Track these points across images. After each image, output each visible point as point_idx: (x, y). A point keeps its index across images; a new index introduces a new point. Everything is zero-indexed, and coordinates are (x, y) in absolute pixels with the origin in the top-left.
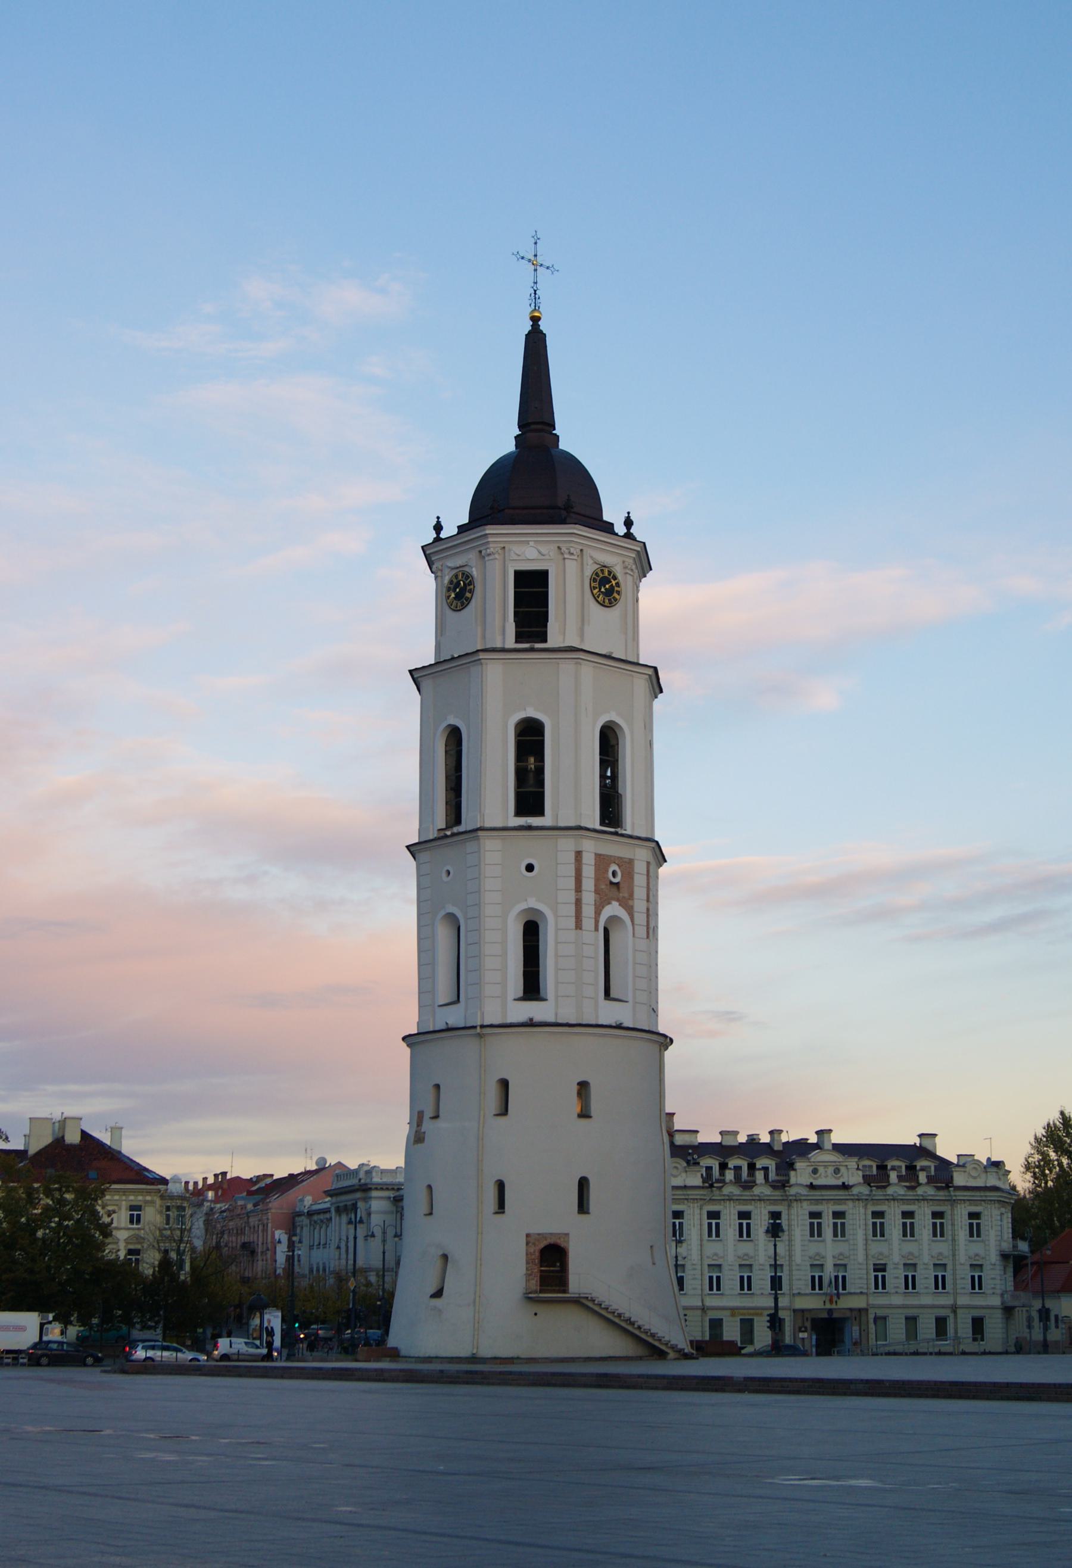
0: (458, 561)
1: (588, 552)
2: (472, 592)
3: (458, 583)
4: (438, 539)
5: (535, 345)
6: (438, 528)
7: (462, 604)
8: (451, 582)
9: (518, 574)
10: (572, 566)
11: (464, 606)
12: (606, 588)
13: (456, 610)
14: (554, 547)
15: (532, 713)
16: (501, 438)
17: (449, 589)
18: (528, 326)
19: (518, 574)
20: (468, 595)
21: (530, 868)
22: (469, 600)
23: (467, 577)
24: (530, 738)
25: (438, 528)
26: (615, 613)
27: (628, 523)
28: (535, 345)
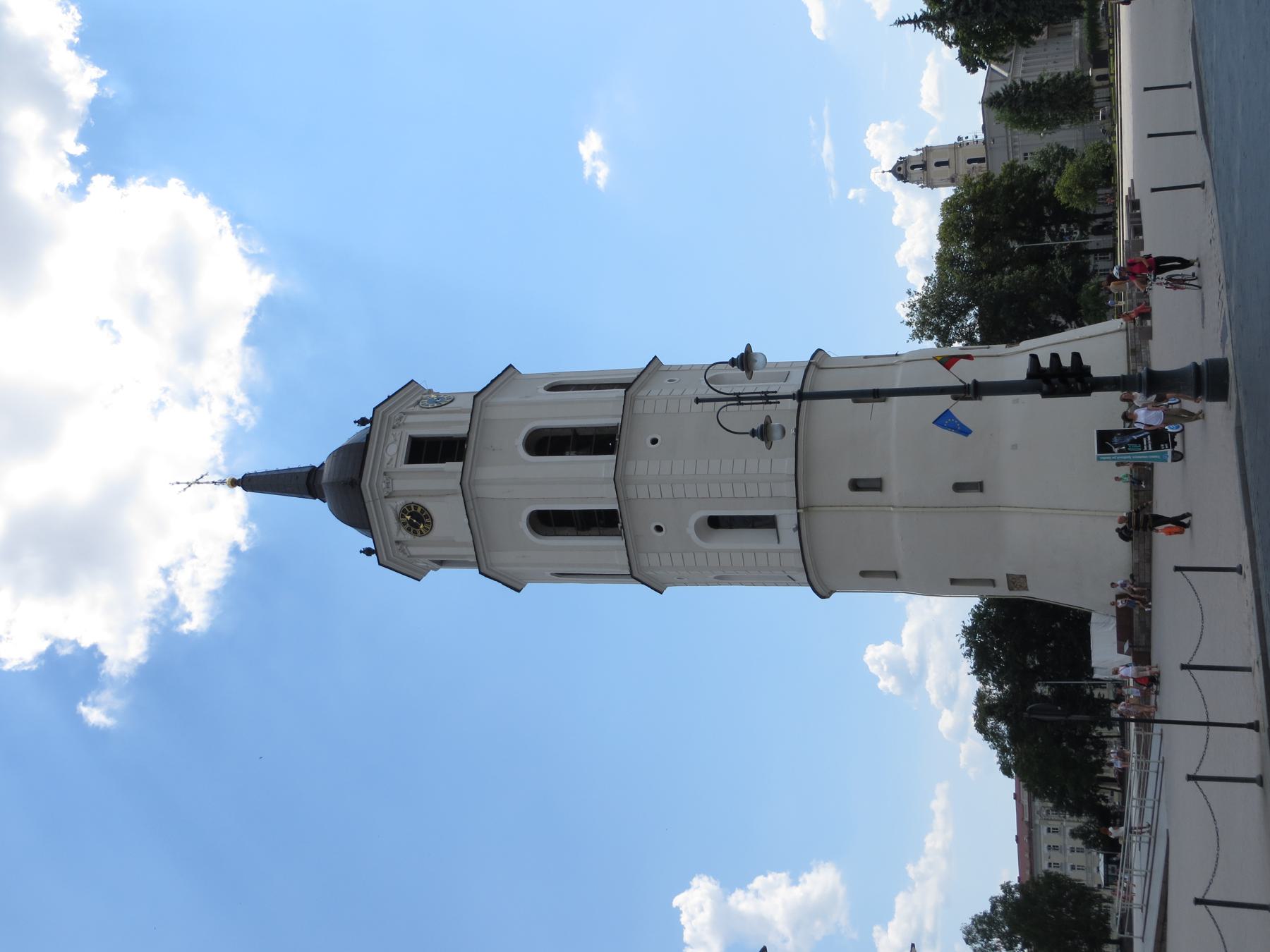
1: (404, 410)
3: (410, 522)
5: (250, 483)
6: (368, 552)
7: (426, 517)
8: (409, 530)
10: (410, 419)
11: (429, 516)
13: (432, 523)
14: (394, 432)
15: (520, 441)
16: (316, 511)
17: (415, 533)
20: (419, 510)
21: (654, 441)
22: (424, 509)
24: (545, 443)
25: (368, 552)
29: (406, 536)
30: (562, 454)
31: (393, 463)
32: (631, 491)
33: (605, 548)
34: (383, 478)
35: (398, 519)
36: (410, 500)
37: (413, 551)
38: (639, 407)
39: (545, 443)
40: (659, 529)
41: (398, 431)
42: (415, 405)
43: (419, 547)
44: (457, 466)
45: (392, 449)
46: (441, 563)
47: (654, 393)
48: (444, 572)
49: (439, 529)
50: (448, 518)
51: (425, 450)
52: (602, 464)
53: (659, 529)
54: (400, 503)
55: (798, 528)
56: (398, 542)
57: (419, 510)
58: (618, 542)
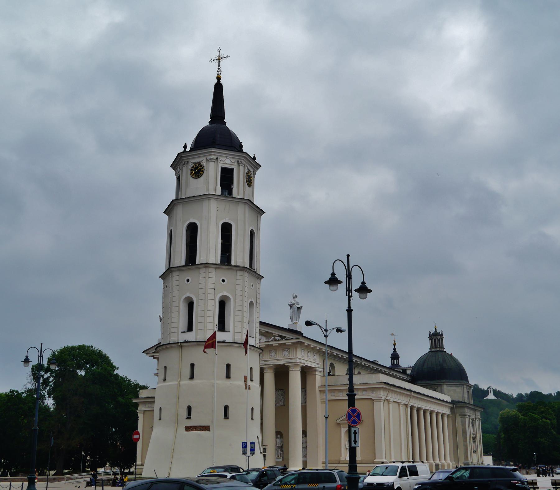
0: (198, 160)
2: (203, 171)
3: (197, 168)
4: (185, 151)
5: (218, 88)
6: (185, 147)
7: (198, 176)
8: (193, 167)
9: (222, 169)
11: (199, 177)
12: (249, 180)
13: (195, 178)
14: (236, 160)
16: (204, 120)
17: (192, 170)
18: (216, 81)
19: (222, 168)
20: (201, 173)
21: (223, 281)
22: (201, 175)
23: (201, 166)
25: (185, 147)
26: (251, 189)
27: (254, 158)
28: (218, 88)
29: (190, 166)
30: (222, 239)
31: (222, 162)
32: (202, 270)
33: (180, 259)
34: (215, 157)
35: (198, 163)
36: (205, 168)
37: (184, 169)
38: (239, 273)
39: (226, 229)
40: (188, 280)
41: (236, 163)
42: (248, 169)
43: (186, 171)
44: (219, 192)
45: (228, 161)
46: (178, 179)
47: (246, 279)
48: (175, 178)
49: (192, 180)
50: (196, 187)
51: (227, 176)
52: (215, 256)
53: (188, 280)
54: (204, 164)
55: (186, 342)
56: (188, 162)
57: (201, 173)
58: (183, 263)
